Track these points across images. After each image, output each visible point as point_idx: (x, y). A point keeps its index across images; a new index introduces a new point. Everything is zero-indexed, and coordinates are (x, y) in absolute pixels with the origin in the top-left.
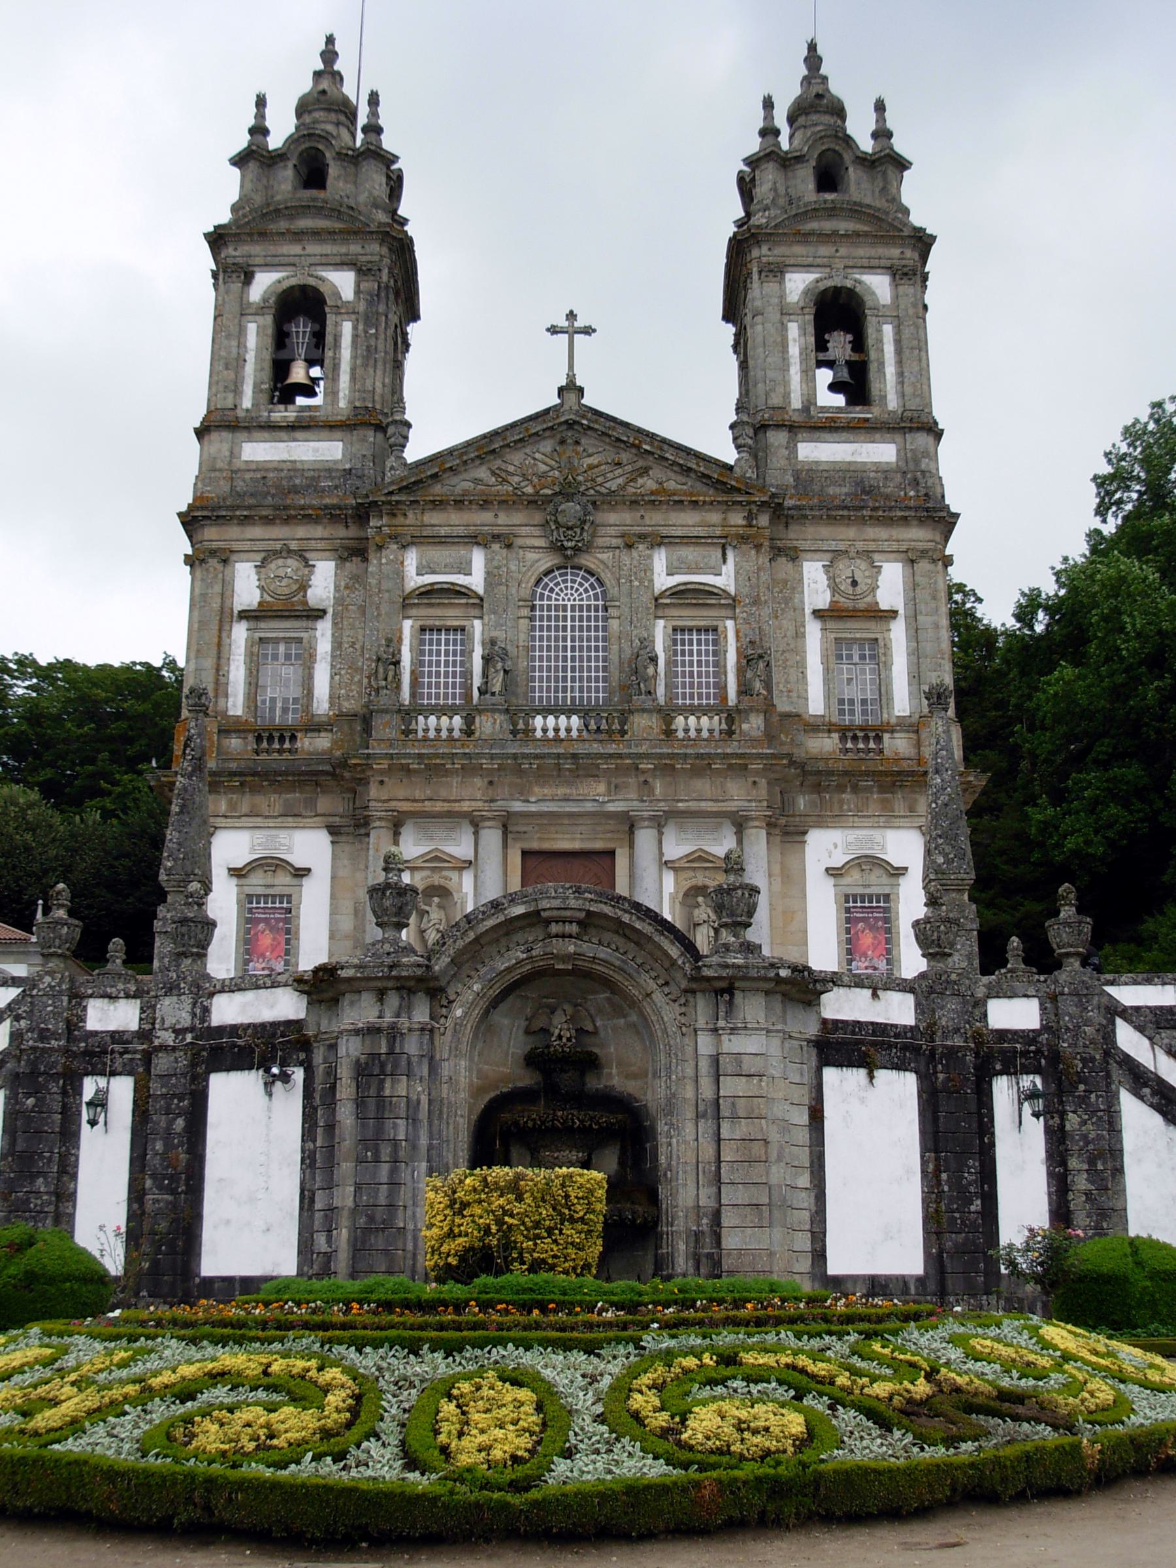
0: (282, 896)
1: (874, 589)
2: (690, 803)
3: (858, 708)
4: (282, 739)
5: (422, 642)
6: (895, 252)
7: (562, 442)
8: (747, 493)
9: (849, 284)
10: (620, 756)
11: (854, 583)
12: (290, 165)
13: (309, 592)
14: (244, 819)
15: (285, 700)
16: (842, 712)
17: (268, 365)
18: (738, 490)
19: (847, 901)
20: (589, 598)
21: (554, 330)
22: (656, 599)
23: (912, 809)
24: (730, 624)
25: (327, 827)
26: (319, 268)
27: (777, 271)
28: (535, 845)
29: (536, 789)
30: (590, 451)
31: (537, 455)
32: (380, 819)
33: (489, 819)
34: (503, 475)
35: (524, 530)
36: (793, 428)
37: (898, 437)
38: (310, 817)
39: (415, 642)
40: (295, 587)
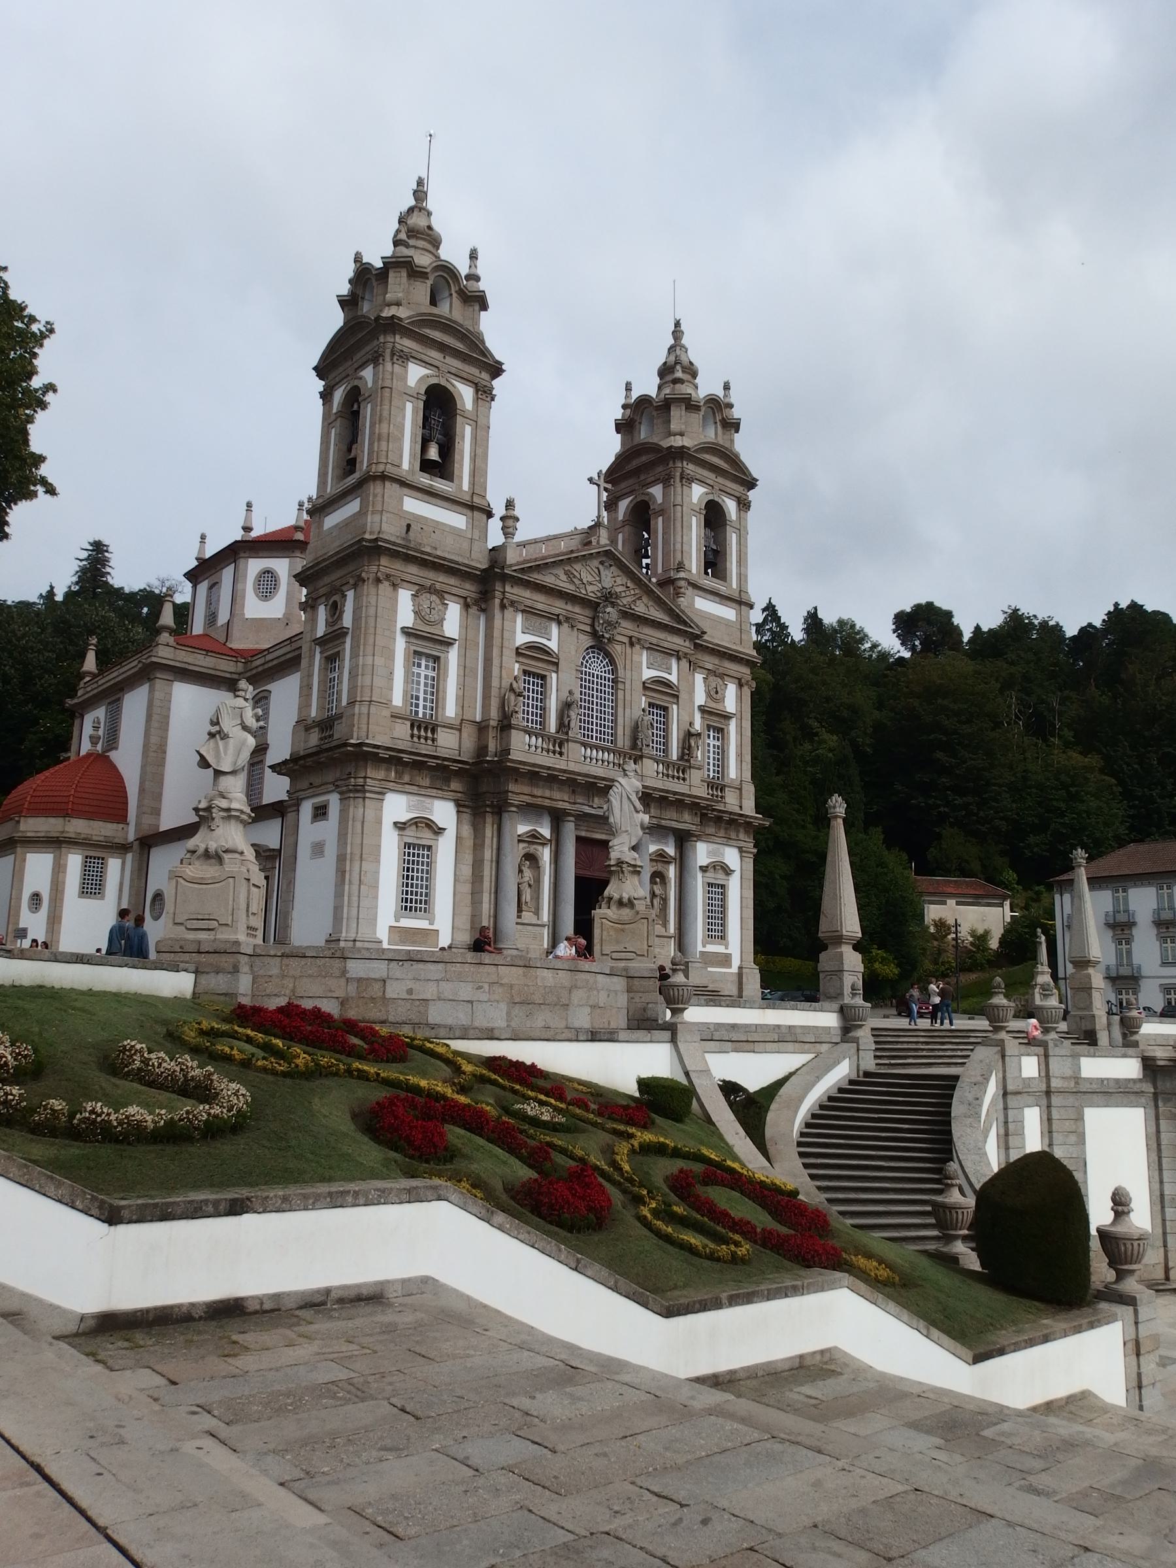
2: (668, 822)
7: (602, 563)
9: (720, 501)
11: (717, 692)
14: (407, 786)
18: (685, 623)
21: (591, 480)
22: (644, 683)
23: (737, 836)
24: (675, 707)
25: (454, 800)
26: (453, 377)
27: (688, 480)
28: (583, 834)
29: (596, 800)
33: (573, 816)
37: (737, 606)
38: (447, 791)
40: (437, 618)
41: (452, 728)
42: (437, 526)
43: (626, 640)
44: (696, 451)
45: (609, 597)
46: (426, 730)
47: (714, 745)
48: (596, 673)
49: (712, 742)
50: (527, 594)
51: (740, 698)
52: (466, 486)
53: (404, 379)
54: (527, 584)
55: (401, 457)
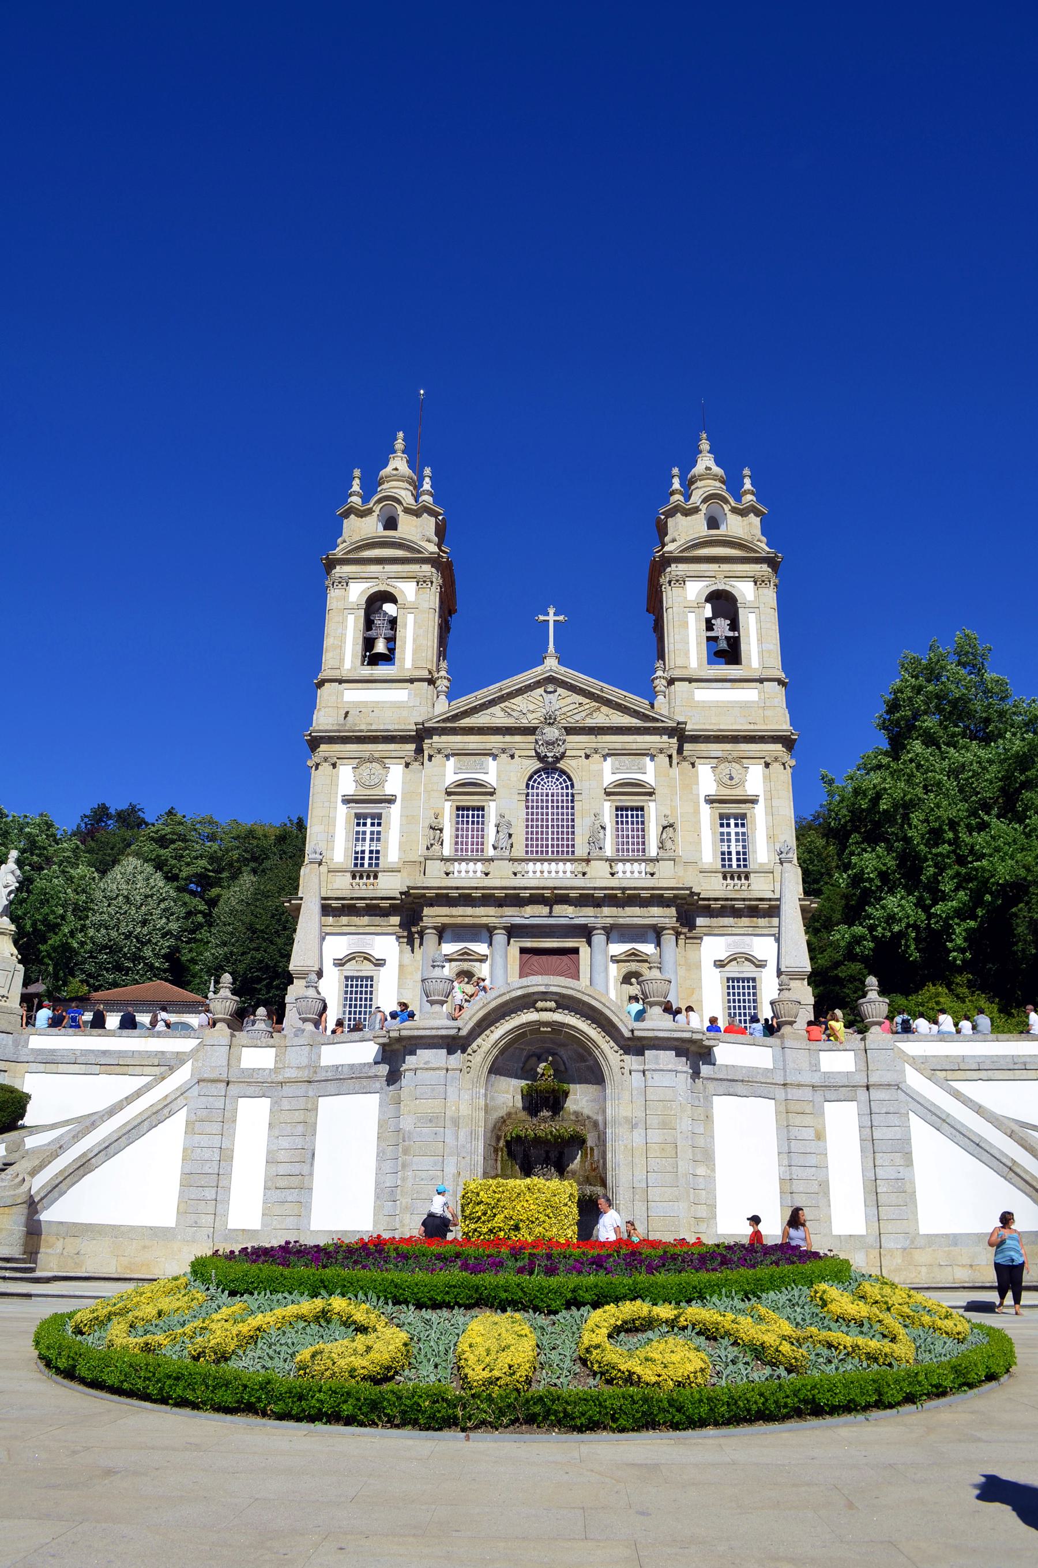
0: (367, 978)
1: (742, 782)
3: (734, 857)
4: (368, 877)
5: (458, 816)
6: (757, 567)
8: (663, 721)
9: (728, 588)
10: (583, 888)
11: (731, 778)
12: (375, 514)
13: (386, 784)
15: (371, 852)
16: (723, 860)
17: (360, 641)
18: (657, 720)
19: (728, 982)
20: (562, 788)
30: (563, 696)
31: (529, 699)
32: (429, 928)
34: (509, 711)
35: (523, 746)
36: (690, 681)
39: (454, 816)
41: (392, 871)
42: (374, 706)
43: (582, 753)
44: (681, 552)
45: (550, 720)
46: (368, 877)
47: (737, 834)
48: (550, 792)
49: (733, 830)
50: (458, 738)
51: (767, 779)
52: (408, 664)
53: (345, 598)
54: (454, 731)
55: (342, 660)
